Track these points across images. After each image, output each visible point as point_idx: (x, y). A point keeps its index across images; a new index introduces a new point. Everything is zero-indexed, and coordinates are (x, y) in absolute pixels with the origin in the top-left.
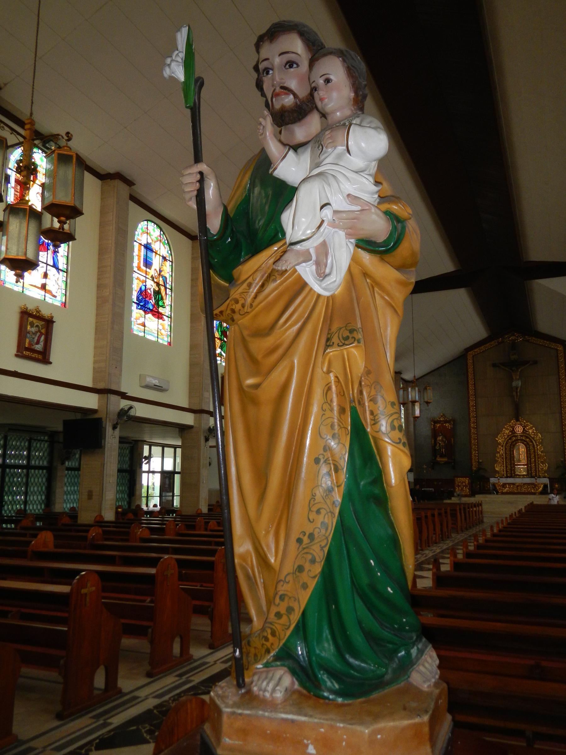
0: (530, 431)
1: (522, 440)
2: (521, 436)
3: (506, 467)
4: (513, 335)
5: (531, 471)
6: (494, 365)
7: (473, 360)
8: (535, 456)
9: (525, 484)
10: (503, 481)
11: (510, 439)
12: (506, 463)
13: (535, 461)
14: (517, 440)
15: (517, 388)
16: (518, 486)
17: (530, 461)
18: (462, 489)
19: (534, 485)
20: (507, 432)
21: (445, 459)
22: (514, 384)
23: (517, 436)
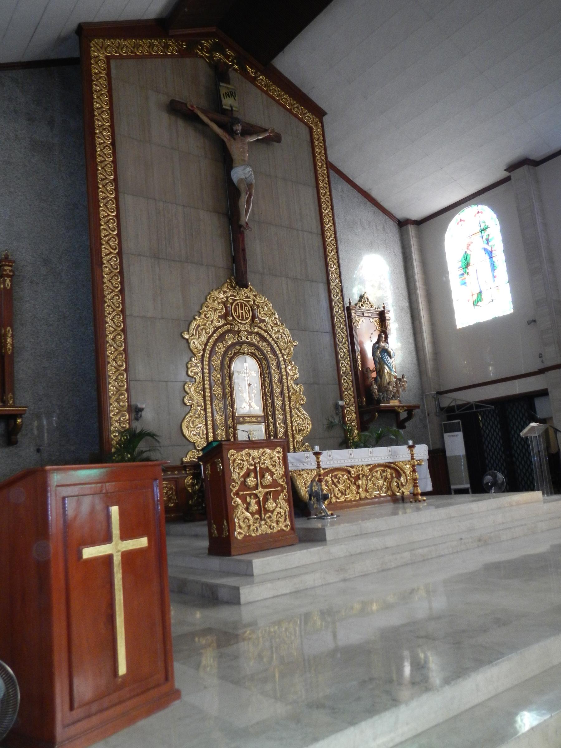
1: (251, 344)
8: (282, 394)
9: (373, 468)
11: (221, 338)
13: (283, 408)
14: (241, 343)
15: (250, 186)
17: (273, 407)
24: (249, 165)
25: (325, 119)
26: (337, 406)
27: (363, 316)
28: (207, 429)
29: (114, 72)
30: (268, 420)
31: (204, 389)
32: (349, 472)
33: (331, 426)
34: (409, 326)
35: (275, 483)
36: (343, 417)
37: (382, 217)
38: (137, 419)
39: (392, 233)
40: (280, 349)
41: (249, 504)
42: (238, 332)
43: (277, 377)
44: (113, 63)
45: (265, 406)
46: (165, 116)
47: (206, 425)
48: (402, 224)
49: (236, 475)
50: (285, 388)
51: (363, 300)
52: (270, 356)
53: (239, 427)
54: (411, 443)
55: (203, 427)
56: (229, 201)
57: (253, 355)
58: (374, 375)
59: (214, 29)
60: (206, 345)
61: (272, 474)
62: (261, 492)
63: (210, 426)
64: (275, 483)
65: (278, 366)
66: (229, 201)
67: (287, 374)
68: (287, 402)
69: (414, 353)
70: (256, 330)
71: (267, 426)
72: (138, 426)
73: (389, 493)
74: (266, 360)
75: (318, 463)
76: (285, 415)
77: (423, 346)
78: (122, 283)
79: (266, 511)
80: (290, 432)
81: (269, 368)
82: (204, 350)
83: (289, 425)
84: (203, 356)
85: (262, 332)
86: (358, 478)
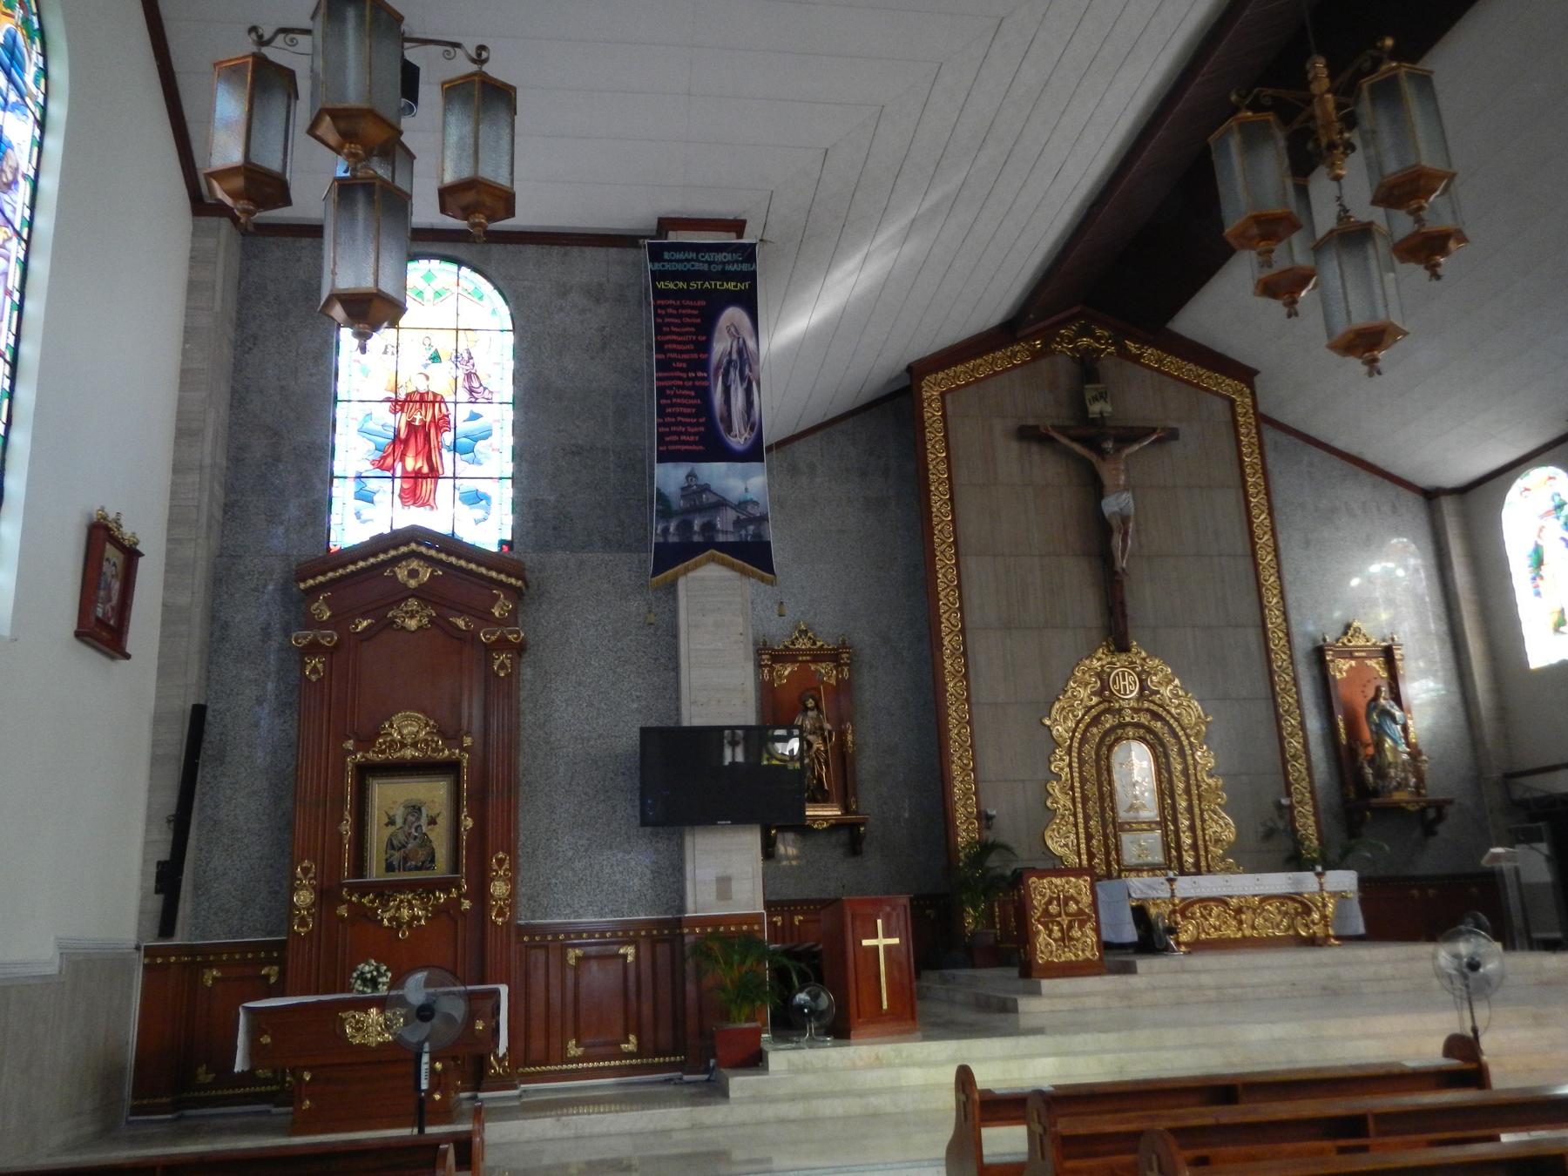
0: (1167, 692)
1: (1138, 725)
2: (1136, 710)
3: (1089, 837)
4: (1085, 331)
5: (1179, 848)
6: (1029, 435)
7: (943, 408)
8: (1188, 791)
10: (1187, 887)
11: (1096, 721)
12: (1087, 818)
13: (1190, 809)
14: (1123, 726)
15: (1125, 520)
16: (1239, 911)
17: (1174, 807)
18: (1066, 938)
19: (1303, 906)
20: (1083, 693)
21: (833, 812)
22: (1111, 505)
23: (1121, 710)
24: (1126, 489)
25: (1257, 380)
26: (1279, 806)
27: (1352, 658)
28: (1078, 838)
29: (949, 408)
30: (1166, 826)
31: (1072, 788)
32: (1227, 904)
33: (1270, 834)
34: (1451, 664)
35: (1080, 912)
36: (1292, 820)
37: (1391, 490)
38: (989, 828)
39: (1413, 508)
40: (1183, 729)
41: (1051, 931)
42: (1121, 710)
43: (1179, 767)
44: (948, 397)
45: (1162, 808)
46: (1015, 445)
47: (1077, 834)
48: (1431, 496)
49: (1038, 901)
50: (1192, 782)
51: (1351, 632)
52: (1167, 738)
53: (1126, 838)
54: (1319, 869)
55: (1072, 836)
56: (1099, 539)
57: (1142, 739)
58: (1371, 750)
59: (1076, 310)
60: (1074, 731)
61: (1077, 903)
62: (1065, 921)
63: (1082, 836)
64: (1080, 912)
65: (1182, 753)
66: (1099, 539)
67: (1196, 763)
68: (1196, 802)
69: (1460, 709)
70: (1146, 705)
71: (1165, 834)
72: (990, 836)
73: (1291, 932)
74: (1162, 745)
75: (1321, 885)
76: (1192, 820)
77: (1475, 697)
78: (966, 665)
79: (1071, 939)
80: (1200, 842)
81: (1167, 756)
82: (1072, 739)
83: (1199, 833)
84: (1070, 746)
85: (1155, 708)
86: (1239, 911)
